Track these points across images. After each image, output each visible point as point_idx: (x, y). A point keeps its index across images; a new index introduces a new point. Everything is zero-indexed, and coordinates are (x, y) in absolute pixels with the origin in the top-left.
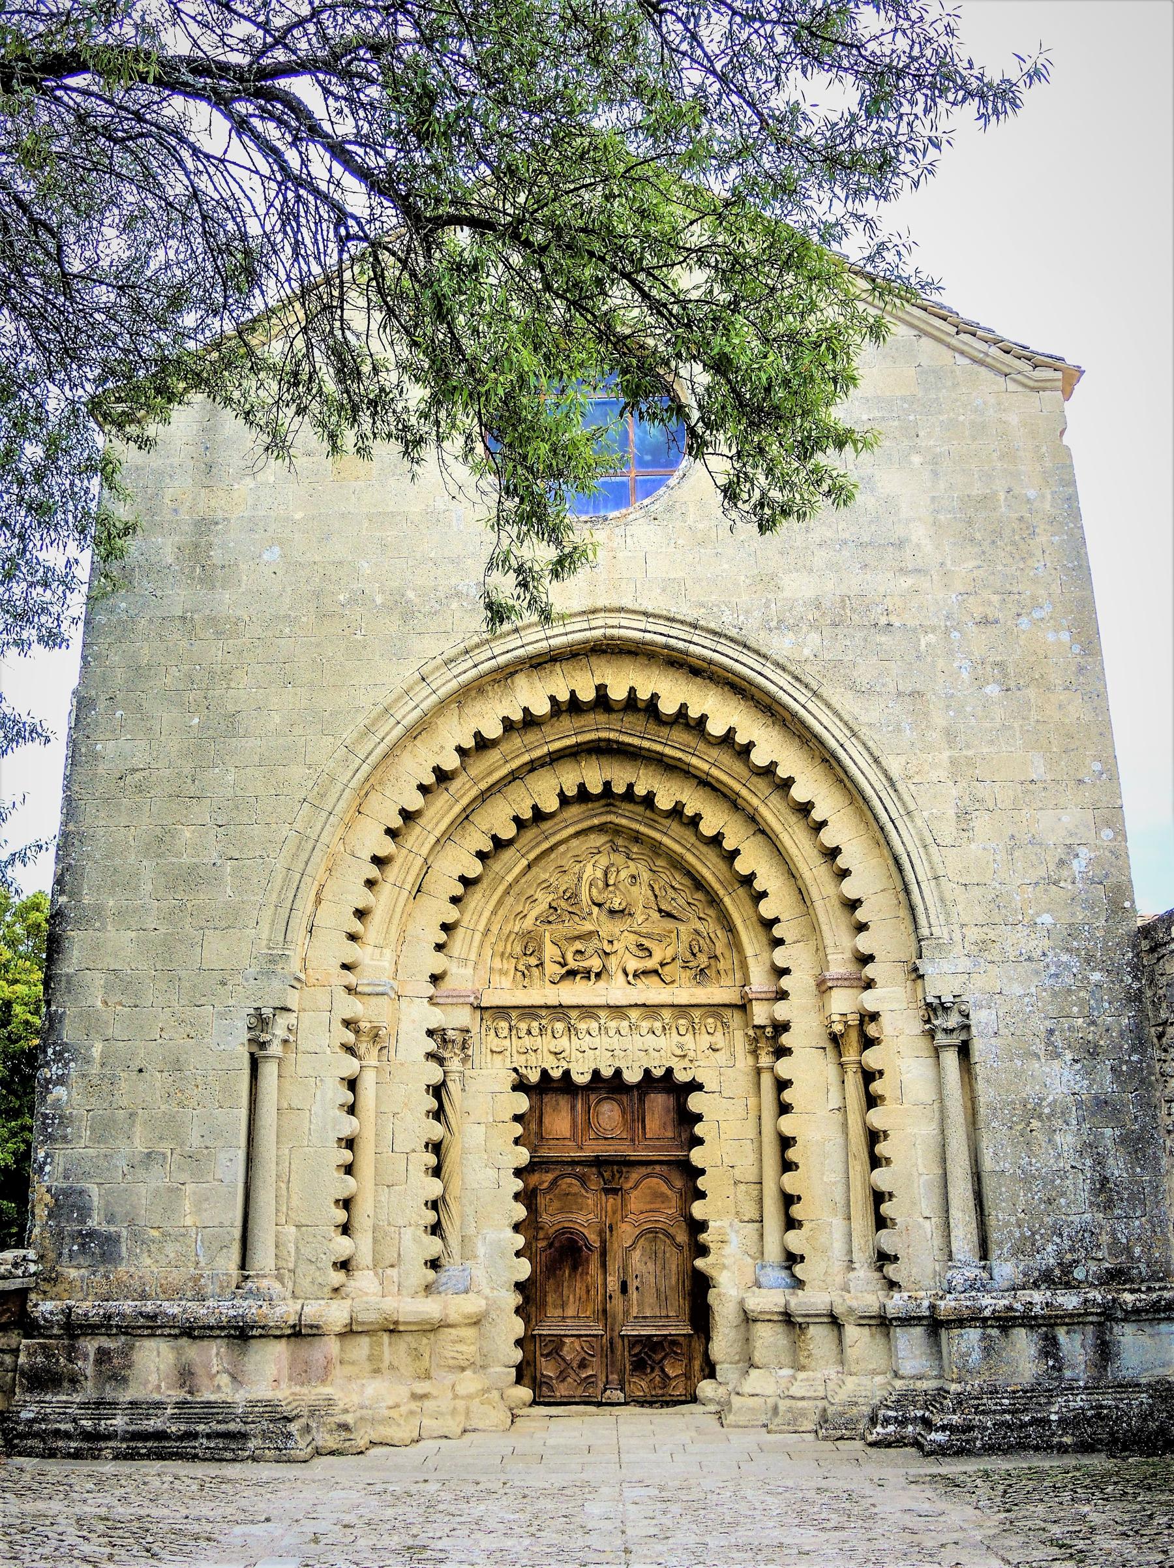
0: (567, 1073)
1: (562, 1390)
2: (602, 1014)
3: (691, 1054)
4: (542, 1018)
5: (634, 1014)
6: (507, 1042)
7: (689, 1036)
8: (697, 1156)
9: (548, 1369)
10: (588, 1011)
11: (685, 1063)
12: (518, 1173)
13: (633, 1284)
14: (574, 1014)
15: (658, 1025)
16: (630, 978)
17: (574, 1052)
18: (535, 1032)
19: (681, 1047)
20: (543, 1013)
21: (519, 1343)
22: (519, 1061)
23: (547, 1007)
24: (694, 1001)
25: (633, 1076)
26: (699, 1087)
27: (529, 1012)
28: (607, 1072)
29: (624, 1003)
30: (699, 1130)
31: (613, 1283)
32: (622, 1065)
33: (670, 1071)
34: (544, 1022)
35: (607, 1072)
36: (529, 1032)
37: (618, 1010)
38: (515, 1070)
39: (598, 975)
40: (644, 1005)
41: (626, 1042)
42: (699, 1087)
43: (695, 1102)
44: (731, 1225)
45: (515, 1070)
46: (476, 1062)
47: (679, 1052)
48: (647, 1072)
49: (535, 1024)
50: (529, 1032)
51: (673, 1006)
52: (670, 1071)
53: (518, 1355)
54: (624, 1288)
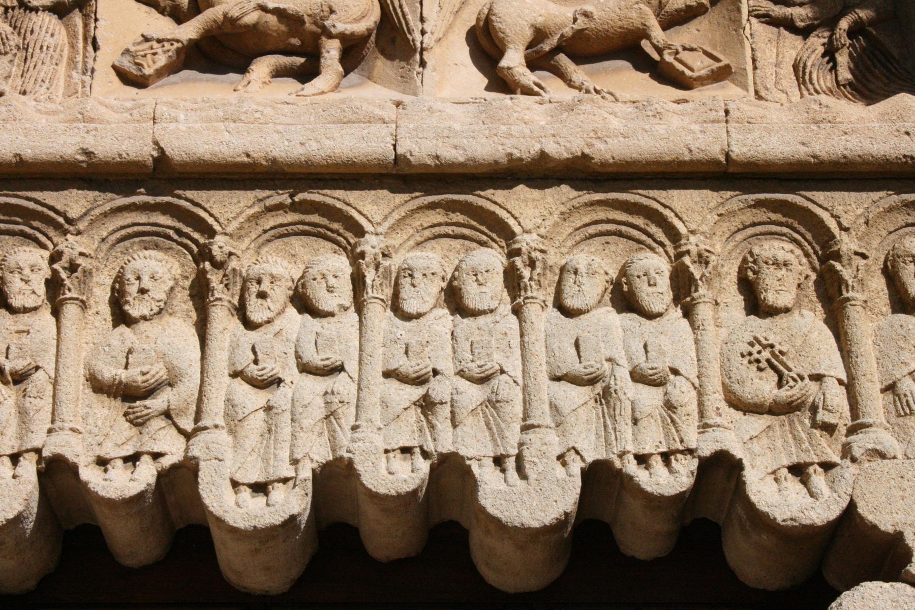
0: (180, 480)
2: (371, 207)
4: (64, 225)
5: (530, 211)
7: (810, 322)
10: (306, 190)
14: (227, 208)
15: (655, 265)
16: (513, 60)
17: (221, 386)
19: (777, 367)
20: (74, 202)
28: (393, 475)
29: (484, 146)
32: (472, 443)
34: (72, 246)
35: (393, 475)
37: (452, 187)
39: (353, 53)
41: (495, 335)
47: (764, 387)
48: (601, 479)
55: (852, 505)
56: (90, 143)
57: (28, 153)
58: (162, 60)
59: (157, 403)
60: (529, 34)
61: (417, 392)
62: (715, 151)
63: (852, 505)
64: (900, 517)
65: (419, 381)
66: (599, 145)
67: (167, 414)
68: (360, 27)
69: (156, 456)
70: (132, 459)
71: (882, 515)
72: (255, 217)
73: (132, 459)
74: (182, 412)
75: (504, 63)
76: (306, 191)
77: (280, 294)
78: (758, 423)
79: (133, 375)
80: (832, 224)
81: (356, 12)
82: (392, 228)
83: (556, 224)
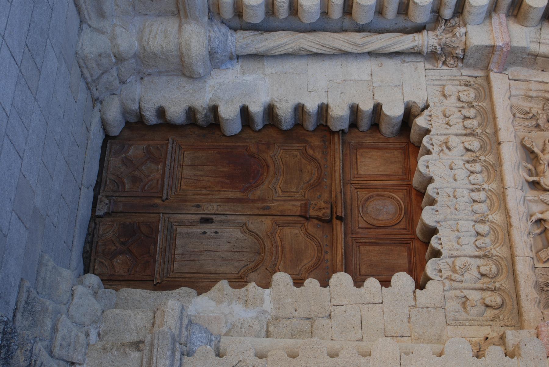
1: (114, 162)
3: (457, 277)
6: (453, 99)
8: (341, 280)
9: (135, 151)
11: (446, 273)
12: (323, 109)
13: (209, 229)
18: (468, 123)
21: (161, 112)
22: (435, 110)
23: (496, 131)
24: (521, 279)
25: (428, 216)
26: (420, 285)
27: (489, 116)
29: (511, 204)
30: (372, 283)
31: (210, 209)
33: (437, 254)
36: (466, 118)
37: (500, 199)
38: (427, 107)
40: (510, 225)
42: (420, 285)
43: (402, 281)
44: (265, 312)
45: (427, 107)
46: (432, 72)
49: (475, 122)
50: (466, 118)
51: (513, 257)
52: (437, 254)
53: (151, 117)
54: (207, 221)
55: (432, 279)
56: (502, 130)
57: (498, 119)
58: (528, 146)
59: (444, 148)
60: (545, 218)
61: (451, 196)
62: (516, 253)
63: (432, 279)
64: (429, 288)
65: (454, 196)
66: (515, 230)
67: (442, 150)
68: (542, 184)
69: (433, 149)
70: (432, 144)
71: (429, 285)
72: (490, 164)
73: (432, 144)
74: (443, 153)
75: (537, 214)
76: (495, 169)
77: (472, 169)
78: (450, 263)
79: (450, 144)
80: (502, 282)
81: (547, 183)
82: (490, 190)
83: (495, 223)
